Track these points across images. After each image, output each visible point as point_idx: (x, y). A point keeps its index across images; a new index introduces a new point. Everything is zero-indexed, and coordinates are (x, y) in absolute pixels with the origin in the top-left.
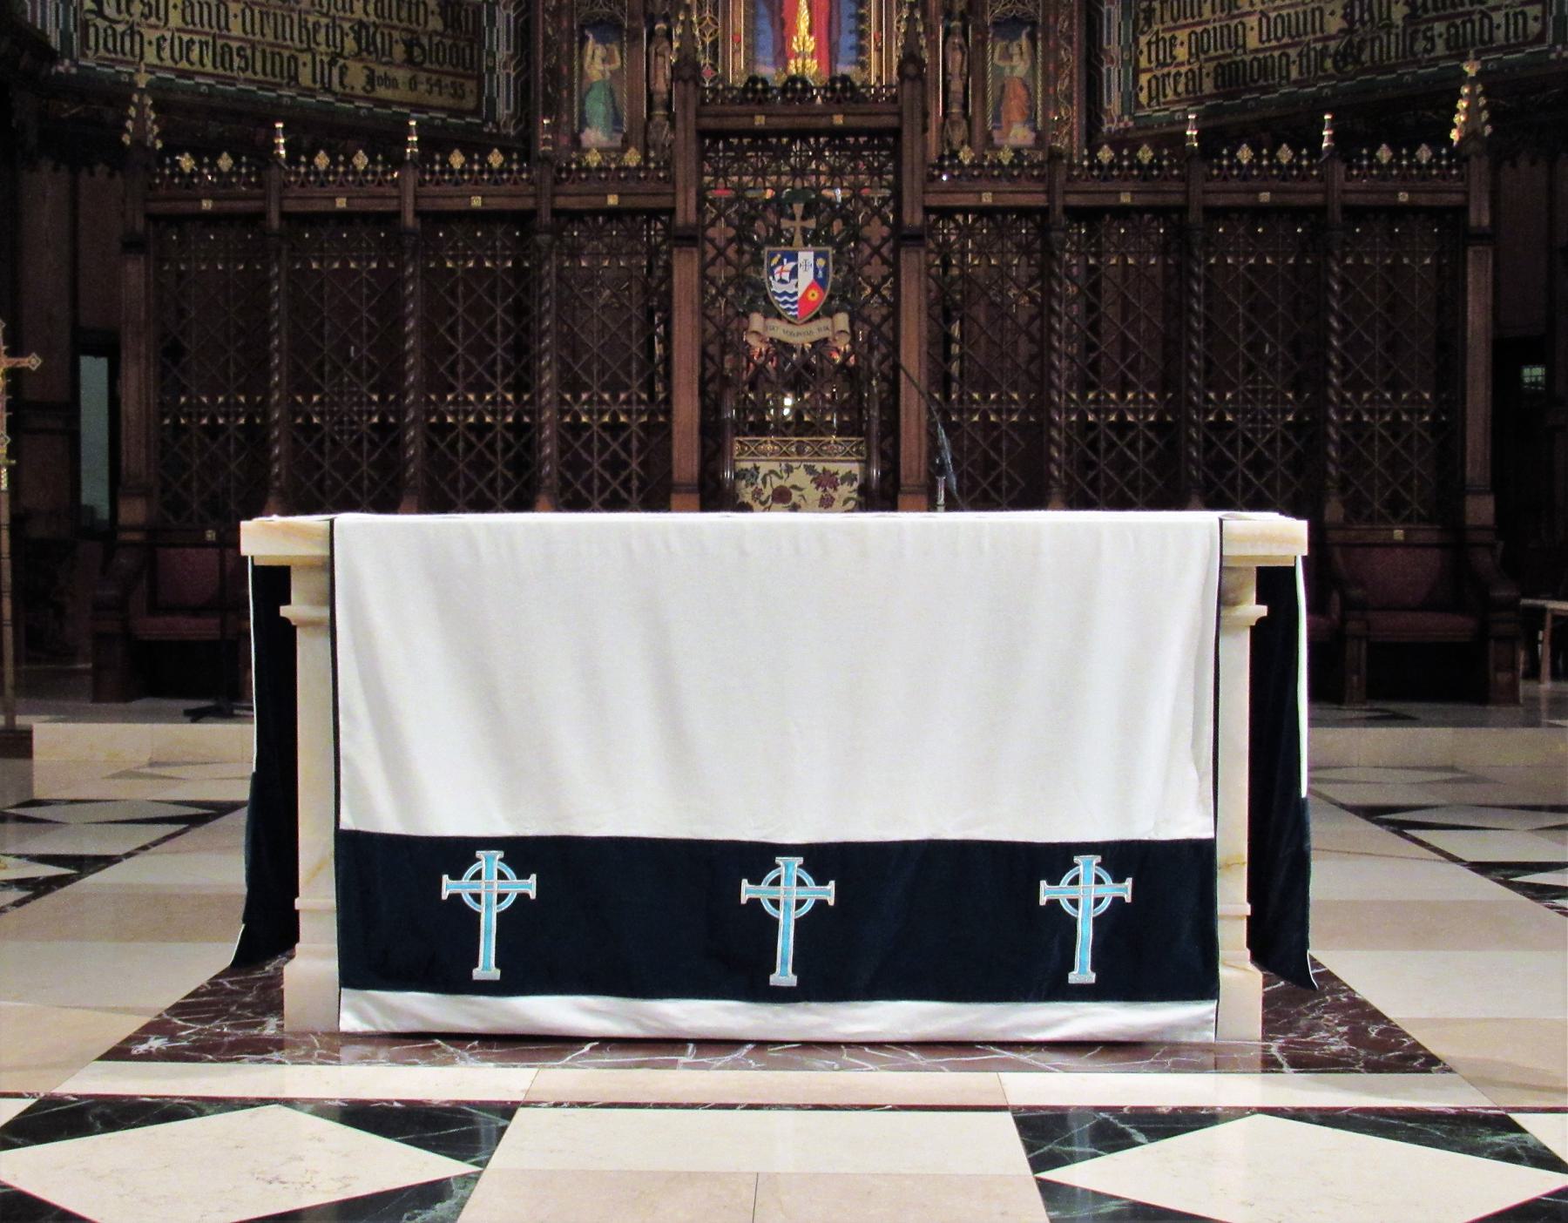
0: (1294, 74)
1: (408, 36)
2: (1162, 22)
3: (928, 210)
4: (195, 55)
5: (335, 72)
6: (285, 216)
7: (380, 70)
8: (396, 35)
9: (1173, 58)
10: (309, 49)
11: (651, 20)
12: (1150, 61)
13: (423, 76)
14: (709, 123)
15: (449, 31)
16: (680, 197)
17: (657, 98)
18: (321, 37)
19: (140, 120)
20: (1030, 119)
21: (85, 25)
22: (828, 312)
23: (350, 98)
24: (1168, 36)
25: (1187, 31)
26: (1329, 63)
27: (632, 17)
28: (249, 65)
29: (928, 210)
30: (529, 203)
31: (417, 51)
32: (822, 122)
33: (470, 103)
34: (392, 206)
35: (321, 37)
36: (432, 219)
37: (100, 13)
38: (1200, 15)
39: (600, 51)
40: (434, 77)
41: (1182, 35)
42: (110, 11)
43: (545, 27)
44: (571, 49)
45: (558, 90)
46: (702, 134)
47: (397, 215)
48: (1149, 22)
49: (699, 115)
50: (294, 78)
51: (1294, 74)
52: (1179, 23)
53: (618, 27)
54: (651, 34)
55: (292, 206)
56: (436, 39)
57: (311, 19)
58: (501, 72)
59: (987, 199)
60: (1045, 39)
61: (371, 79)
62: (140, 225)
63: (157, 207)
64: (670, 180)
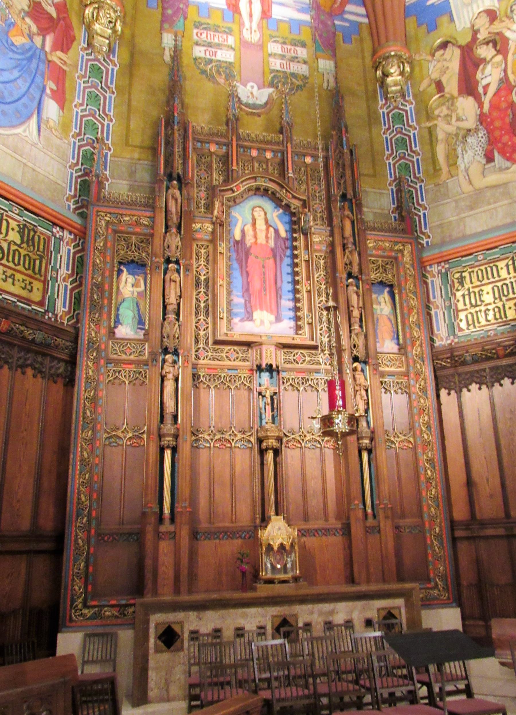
2: (471, 283)
9: (483, 301)
12: (465, 305)
15: (24, 245)
17: (170, 308)
24: (476, 290)
25: (491, 286)
38: (499, 276)
39: (131, 279)
40: (10, 272)
41: (488, 288)
45: (102, 297)
48: (461, 283)
52: (484, 282)
56: (13, 247)
60: (400, 293)
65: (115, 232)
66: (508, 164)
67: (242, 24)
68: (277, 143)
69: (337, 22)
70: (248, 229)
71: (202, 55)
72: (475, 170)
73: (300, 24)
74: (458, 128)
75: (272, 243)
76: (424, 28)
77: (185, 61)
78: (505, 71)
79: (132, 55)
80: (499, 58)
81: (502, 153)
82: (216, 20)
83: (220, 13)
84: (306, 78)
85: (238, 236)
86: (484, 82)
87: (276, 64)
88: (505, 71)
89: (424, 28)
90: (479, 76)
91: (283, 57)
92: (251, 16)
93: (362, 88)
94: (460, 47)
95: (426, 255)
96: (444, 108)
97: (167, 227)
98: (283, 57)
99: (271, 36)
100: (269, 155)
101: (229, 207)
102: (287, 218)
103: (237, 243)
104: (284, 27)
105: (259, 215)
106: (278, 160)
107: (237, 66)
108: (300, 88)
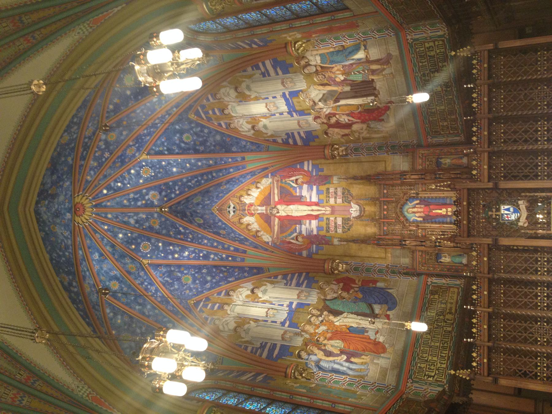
0: (451, 97)
1: (439, 304)
3: (489, 181)
4: (444, 355)
5: (448, 321)
6: (489, 341)
7: (448, 311)
8: (439, 306)
10: (443, 327)
11: (436, 246)
13: (449, 301)
14: (465, 235)
16: (485, 242)
17: (455, 245)
18: (440, 324)
19: (463, 374)
20: (461, 158)
21: (436, 380)
22: (518, 206)
23: (455, 319)
26: (448, 89)
27: (435, 250)
28: (446, 342)
29: (489, 181)
30: (486, 280)
31: (443, 301)
32: (466, 207)
33: (456, 290)
34: (486, 314)
35: (440, 324)
36: (490, 304)
37: (434, 377)
40: (450, 298)
42: (433, 374)
43: (438, 271)
44: (443, 265)
45: (453, 269)
46: (468, 236)
47: (489, 313)
49: (464, 237)
50: (450, 332)
51: (451, 97)
53: (437, 254)
54: (439, 246)
55: (486, 339)
57: (435, 326)
58: (448, 282)
59: (486, 167)
61: (450, 313)
62: (490, 378)
63: (486, 374)
64: (480, 245)
65: (425, 263)
66: (386, 115)
67: (324, 214)
68: (380, 203)
69: (314, 174)
70: (417, 215)
71: (341, 230)
73: (318, 190)
74: (366, 130)
75: (423, 206)
76: (316, 140)
77: (344, 236)
78: (343, 114)
79: (347, 256)
80: (337, 116)
81: (381, 116)
82: (324, 224)
83: (320, 223)
84: (343, 189)
85: (421, 219)
86: (347, 121)
87: (339, 201)
88: (343, 114)
89: (316, 140)
90: (344, 123)
91: (335, 198)
92: (319, 210)
93: (344, 164)
94: (329, 128)
95: (423, 143)
96: (355, 134)
97: (422, 246)
98: (335, 198)
99: (327, 202)
100: (385, 207)
101: (410, 222)
102: (411, 200)
103: (424, 220)
104: (322, 197)
106: (387, 203)
107: (343, 216)
108: (349, 191)
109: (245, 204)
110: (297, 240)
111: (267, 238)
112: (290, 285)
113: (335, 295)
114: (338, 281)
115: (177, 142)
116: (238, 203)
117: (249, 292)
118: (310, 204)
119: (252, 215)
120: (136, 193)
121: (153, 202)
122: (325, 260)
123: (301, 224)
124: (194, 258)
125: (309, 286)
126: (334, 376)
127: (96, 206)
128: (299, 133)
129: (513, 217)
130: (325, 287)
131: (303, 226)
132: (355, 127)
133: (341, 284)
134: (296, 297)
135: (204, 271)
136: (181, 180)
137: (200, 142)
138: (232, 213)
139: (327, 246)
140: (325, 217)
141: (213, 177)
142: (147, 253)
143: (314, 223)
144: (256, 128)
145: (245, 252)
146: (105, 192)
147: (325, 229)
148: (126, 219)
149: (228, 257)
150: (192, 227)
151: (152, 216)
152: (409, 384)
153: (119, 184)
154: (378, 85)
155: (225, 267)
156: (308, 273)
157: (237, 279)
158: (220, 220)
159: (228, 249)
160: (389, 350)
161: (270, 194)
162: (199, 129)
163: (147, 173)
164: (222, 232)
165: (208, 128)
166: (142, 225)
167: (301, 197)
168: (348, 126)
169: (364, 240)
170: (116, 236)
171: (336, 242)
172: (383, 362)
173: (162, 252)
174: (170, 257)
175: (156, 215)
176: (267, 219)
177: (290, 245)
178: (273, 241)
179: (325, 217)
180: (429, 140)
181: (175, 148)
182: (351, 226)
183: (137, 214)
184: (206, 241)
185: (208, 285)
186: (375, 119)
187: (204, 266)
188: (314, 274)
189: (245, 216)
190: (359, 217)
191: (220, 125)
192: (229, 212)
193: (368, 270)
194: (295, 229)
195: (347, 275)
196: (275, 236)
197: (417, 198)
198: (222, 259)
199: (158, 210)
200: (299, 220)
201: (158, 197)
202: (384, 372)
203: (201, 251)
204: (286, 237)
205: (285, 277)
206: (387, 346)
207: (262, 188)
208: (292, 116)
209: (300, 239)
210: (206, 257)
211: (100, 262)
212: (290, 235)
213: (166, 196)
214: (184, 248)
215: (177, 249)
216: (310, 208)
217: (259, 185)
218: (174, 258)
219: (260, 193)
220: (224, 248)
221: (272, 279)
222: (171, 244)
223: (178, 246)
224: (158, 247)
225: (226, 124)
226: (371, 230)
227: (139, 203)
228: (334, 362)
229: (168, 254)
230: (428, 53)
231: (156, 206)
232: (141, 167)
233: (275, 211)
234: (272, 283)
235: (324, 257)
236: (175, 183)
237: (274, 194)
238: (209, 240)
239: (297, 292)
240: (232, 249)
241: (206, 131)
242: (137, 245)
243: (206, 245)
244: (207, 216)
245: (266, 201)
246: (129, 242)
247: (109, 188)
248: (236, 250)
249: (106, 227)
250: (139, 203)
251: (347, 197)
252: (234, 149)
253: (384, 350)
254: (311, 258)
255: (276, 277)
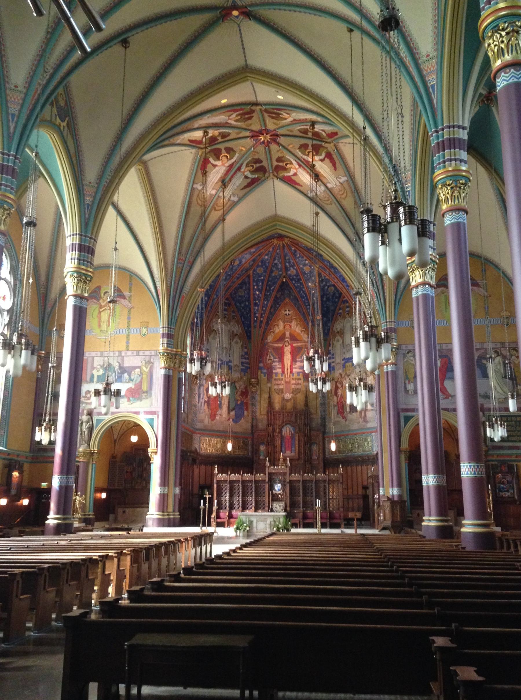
67: (285, 377)
72: (335, 416)
77: (273, 390)
87: (293, 386)
91: (295, 384)
98: (295, 384)
105: (288, 428)
109: (291, 322)
110: (269, 359)
111: (270, 339)
112: (242, 359)
113: (238, 388)
114: (246, 388)
115: (328, 284)
116: (292, 317)
117: (235, 332)
118: (291, 368)
119: (284, 327)
120: (293, 263)
121: (289, 271)
122: (257, 379)
123: (279, 362)
124: (254, 297)
125: (242, 370)
126: (197, 396)
127: (283, 245)
128: (333, 362)
129: (276, 488)
130: (242, 380)
131: (277, 364)
132: (335, 398)
133: (244, 390)
134: (235, 364)
135: (247, 303)
136: (304, 288)
137: (329, 298)
138: (285, 313)
139: (266, 380)
140: (283, 377)
141: (307, 306)
142: (256, 272)
143: (280, 371)
144: (338, 335)
145: (260, 327)
146: (293, 249)
147: (276, 378)
148: (277, 258)
149: (257, 317)
150: (274, 294)
151: (280, 271)
152: (198, 435)
153: (298, 255)
154: (354, 414)
155: (250, 316)
156: (249, 368)
157: (243, 322)
158: (280, 305)
159: (261, 317)
160: (213, 422)
161: (298, 340)
162: (337, 295)
163: (307, 269)
164: (273, 309)
165: (338, 301)
166: (273, 267)
167: (296, 362)
168: (336, 394)
169: (270, 404)
170: (266, 255)
171: (269, 385)
172: (207, 421)
173: (258, 280)
174: (255, 284)
175: (281, 273)
176: (282, 338)
177: (266, 355)
178: (268, 343)
179: (283, 377)
180: (327, 439)
181: (324, 283)
182: (279, 394)
183: (281, 263)
184: (266, 303)
185: (238, 304)
186: (339, 410)
187: (250, 304)
188: (249, 372)
189: (284, 322)
190: (283, 398)
191: (340, 309)
192: (286, 311)
193: (253, 405)
194: (275, 358)
195: (250, 393)
196: (271, 344)
197: (295, 432)
198: (255, 314)
199: (284, 274)
200: (281, 360)
201: (292, 274)
202: (202, 421)
203: (259, 301)
204: (271, 352)
205: (246, 353)
206: (215, 421)
207: (302, 334)
208: (343, 360)
209: (270, 362)
210: (256, 304)
211: (250, 253)
212: (272, 354)
213: (293, 278)
214: (261, 291)
215: (260, 287)
216: (289, 368)
217: (303, 332)
218: (254, 286)
219: (298, 334)
220: (262, 314)
221: (244, 345)
222: (263, 284)
223: (262, 288)
224: (261, 276)
225: (341, 313)
226: (277, 406)
227: (287, 264)
228: (204, 394)
229: (257, 283)
230: (366, 443)
231: (286, 274)
232: (310, 266)
233: (287, 344)
234: (242, 346)
235: (259, 378)
236: (301, 284)
237: (298, 343)
238: (267, 304)
239: (238, 364)
240: (262, 319)
241: (336, 300)
242: (262, 266)
243: (264, 303)
244: (282, 297)
245: (293, 338)
246: (263, 262)
247: (295, 251)
248: (261, 322)
249: (271, 250)
250: (287, 264)
251: (296, 391)
252: (325, 319)
253: (212, 420)
254: (258, 369)
255: (246, 348)
